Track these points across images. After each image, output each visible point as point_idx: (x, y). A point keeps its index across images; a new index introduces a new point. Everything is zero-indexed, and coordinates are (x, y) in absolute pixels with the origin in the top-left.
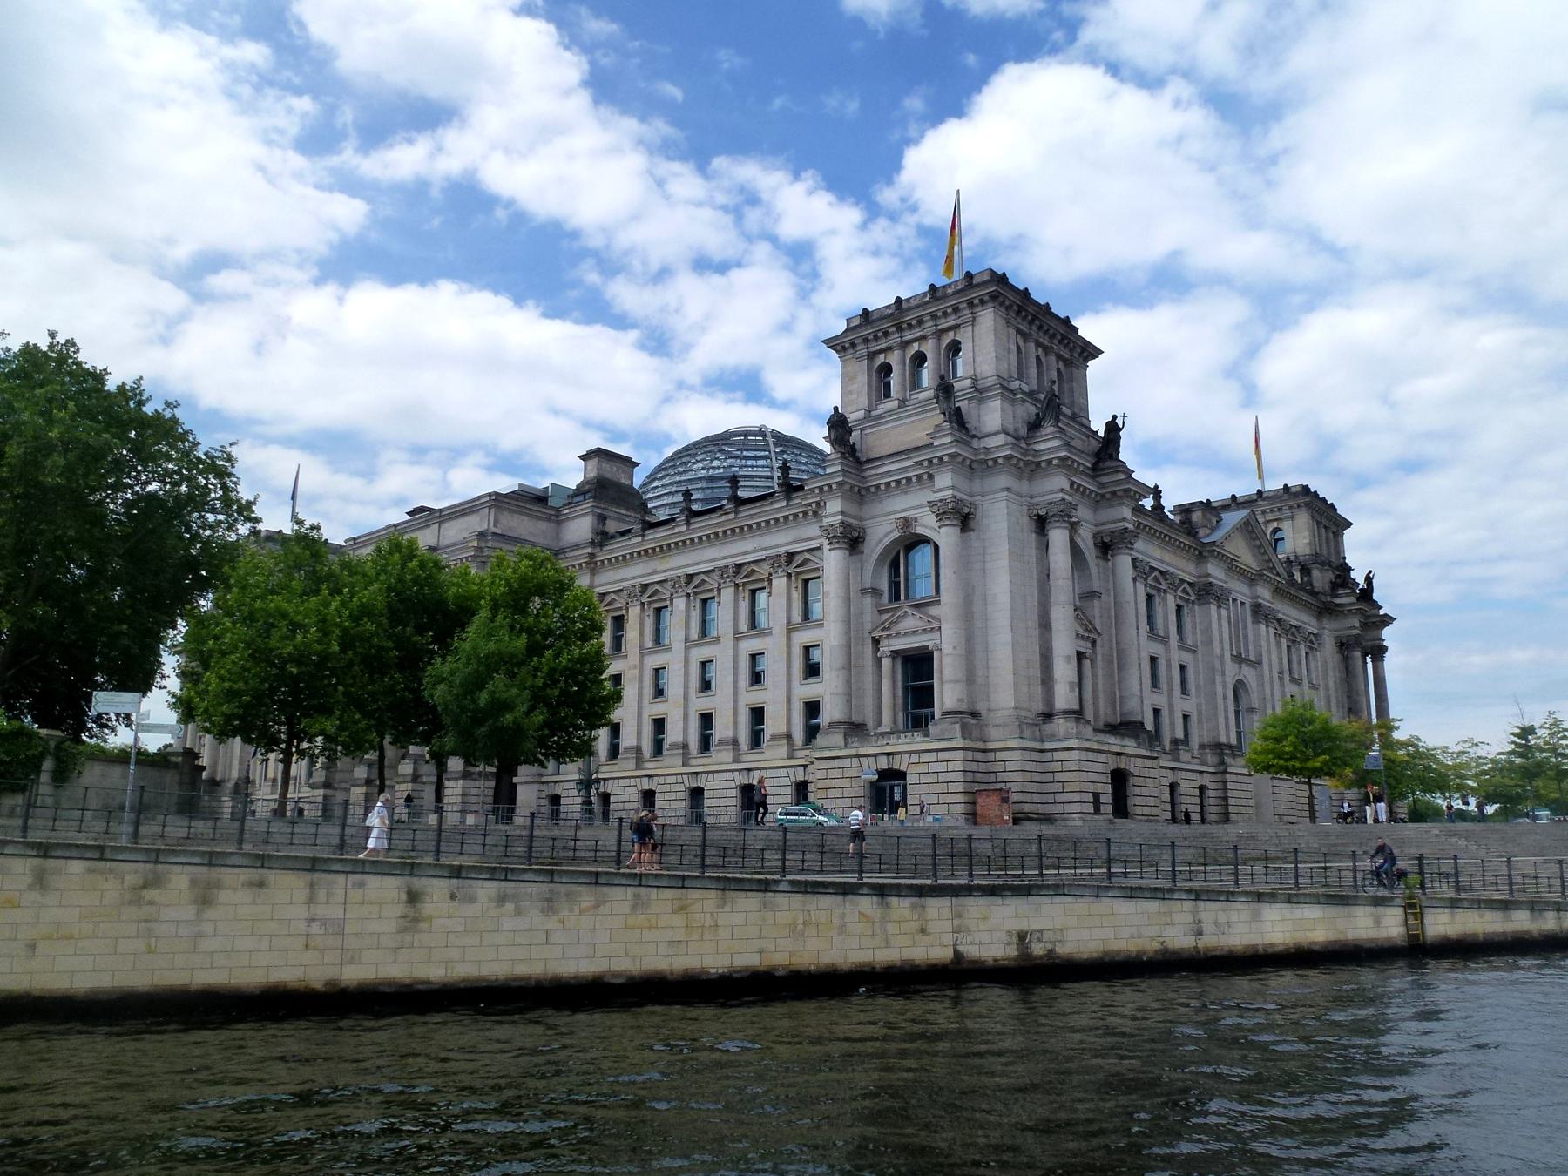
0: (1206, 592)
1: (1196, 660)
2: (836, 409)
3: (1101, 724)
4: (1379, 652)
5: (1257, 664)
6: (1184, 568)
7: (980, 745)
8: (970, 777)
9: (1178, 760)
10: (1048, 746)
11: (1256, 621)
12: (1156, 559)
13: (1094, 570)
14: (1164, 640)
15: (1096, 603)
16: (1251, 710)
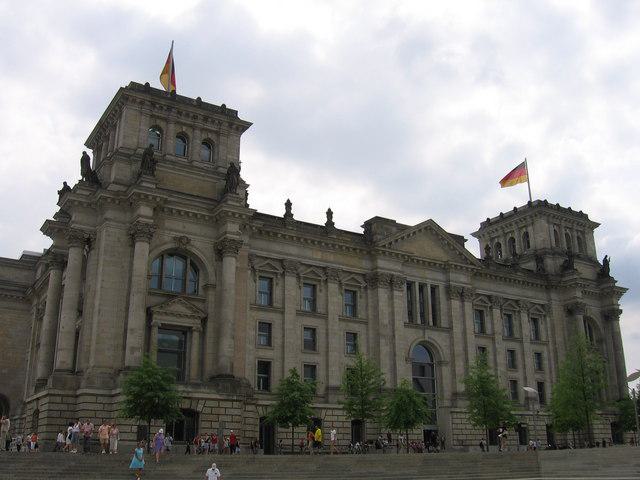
0: (373, 280)
1: (367, 330)
2: (65, 183)
3: (207, 376)
4: (612, 315)
5: (450, 329)
6: (361, 265)
7: (70, 393)
8: (55, 414)
9: (327, 402)
10: (114, 392)
11: (449, 298)
12: (316, 259)
13: (210, 269)
14: (325, 317)
15: (211, 292)
16: (440, 363)
